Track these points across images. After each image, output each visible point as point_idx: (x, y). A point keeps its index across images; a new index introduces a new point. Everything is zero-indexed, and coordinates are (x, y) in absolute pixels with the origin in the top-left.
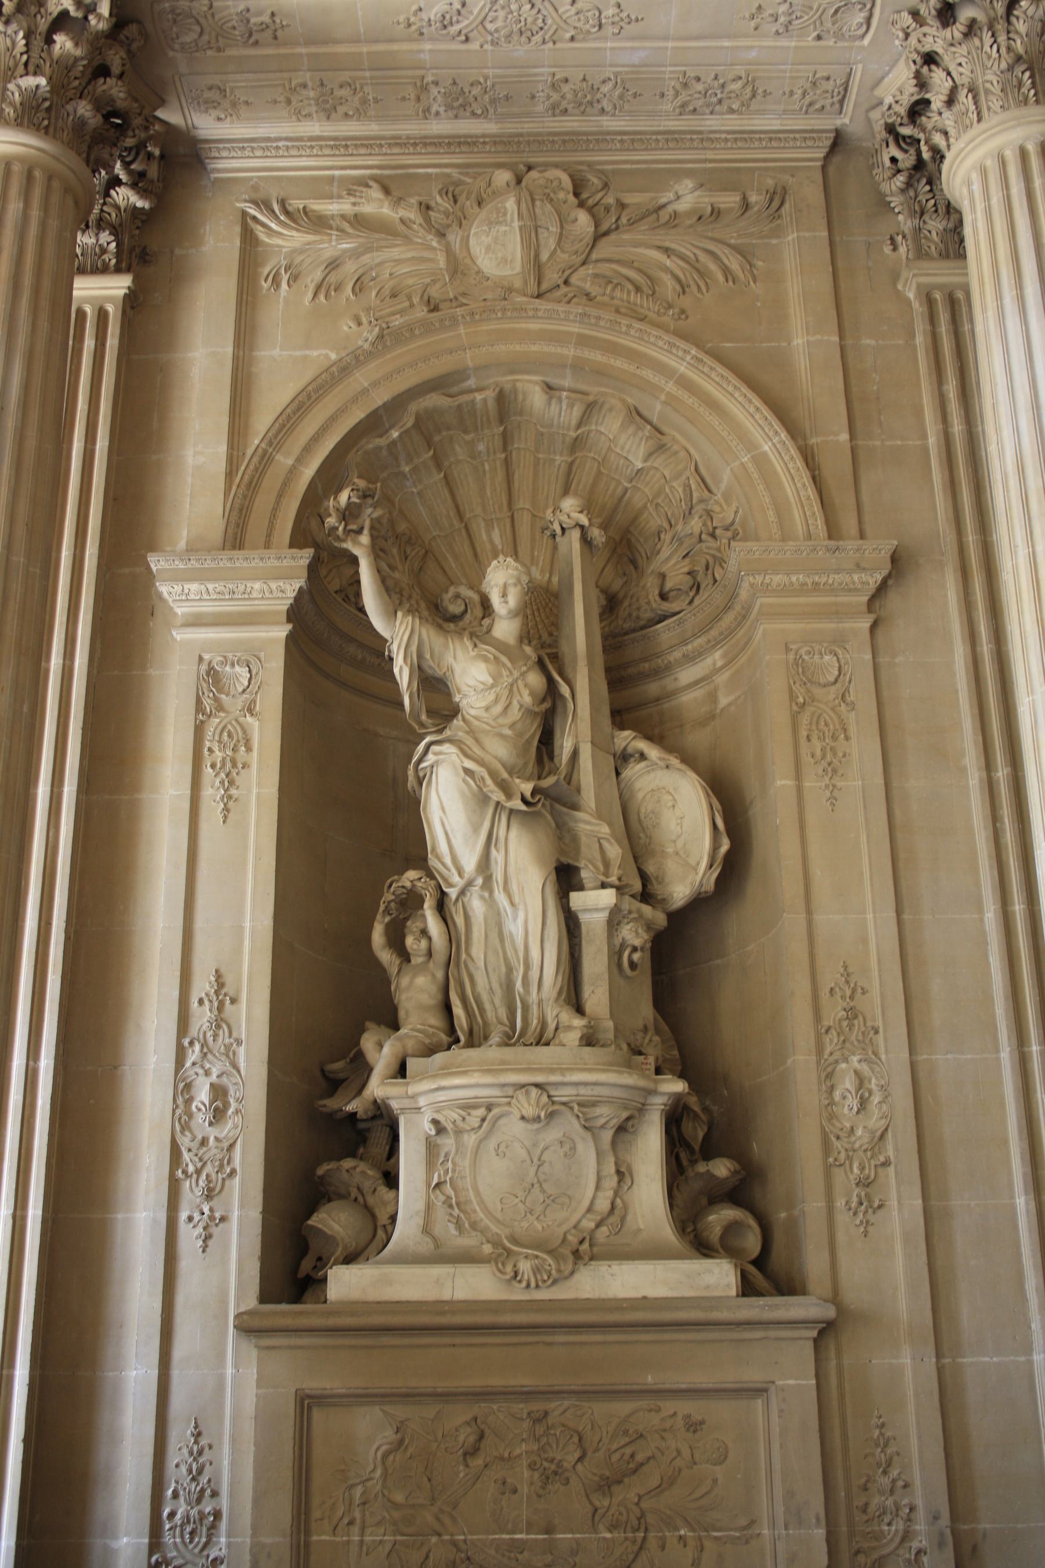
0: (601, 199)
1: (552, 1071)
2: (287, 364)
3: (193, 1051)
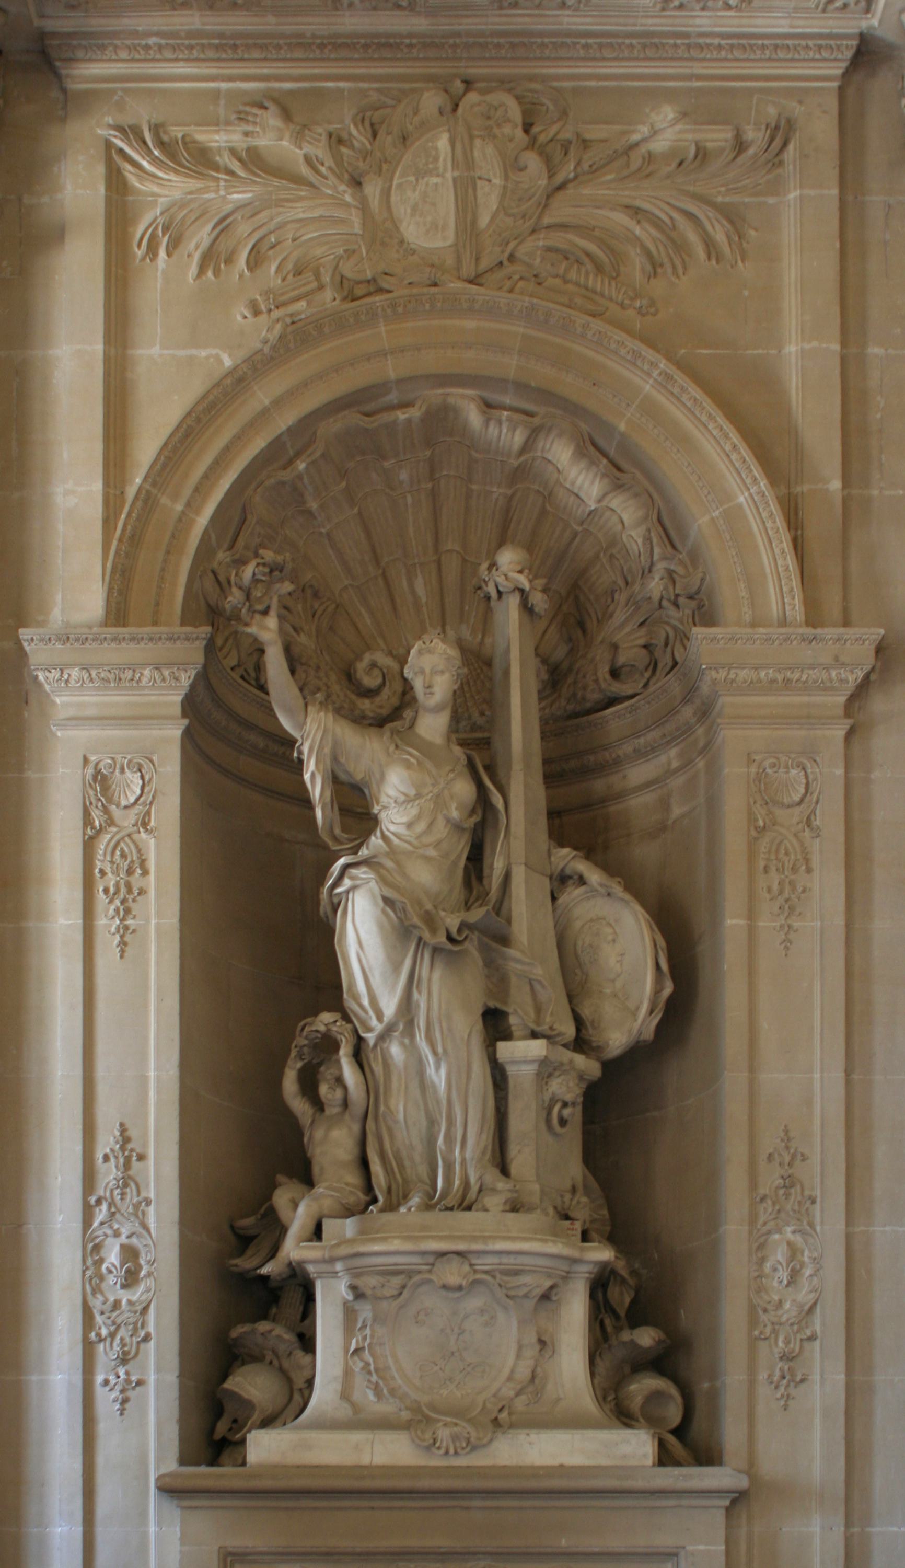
0: (556, 135)
1: (474, 1239)
2: (173, 371)
3: (100, 1210)
